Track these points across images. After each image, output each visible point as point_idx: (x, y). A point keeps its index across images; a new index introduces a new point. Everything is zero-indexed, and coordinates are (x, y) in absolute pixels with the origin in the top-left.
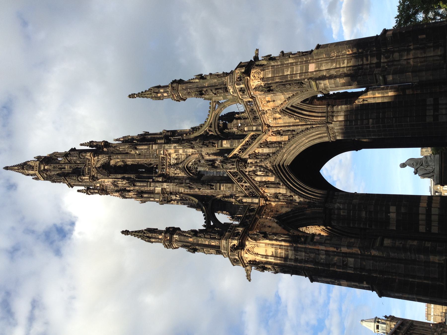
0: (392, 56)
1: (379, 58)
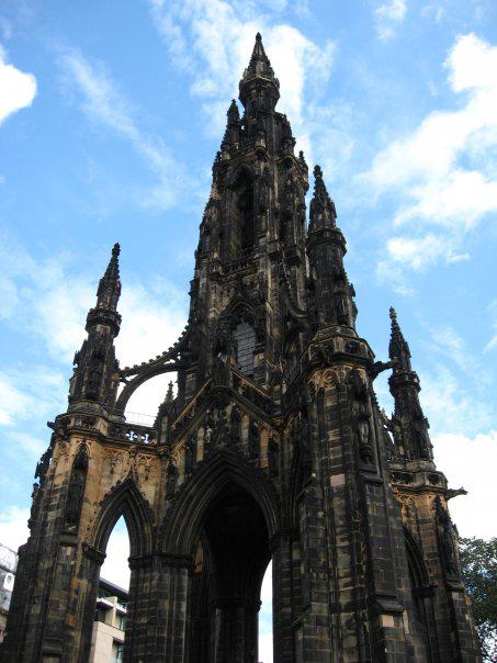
1: (348, 608)
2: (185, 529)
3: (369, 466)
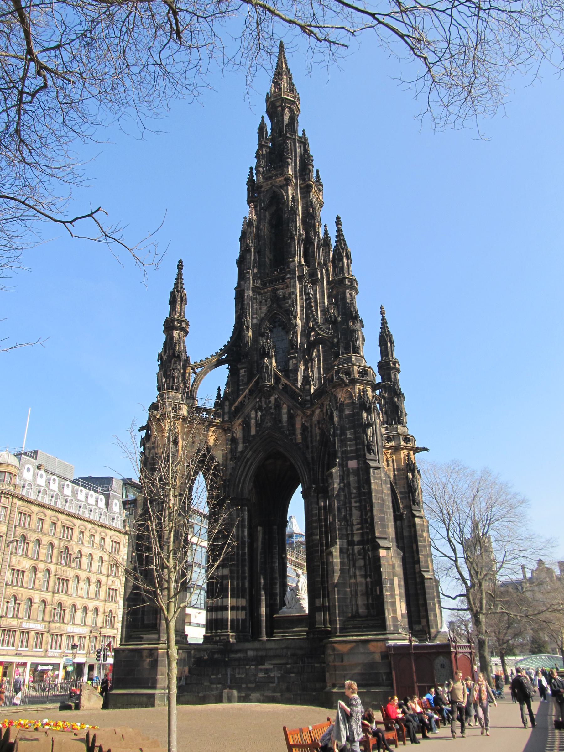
0: (360, 559)
1: (359, 543)
2: (244, 480)
3: (372, 456)
